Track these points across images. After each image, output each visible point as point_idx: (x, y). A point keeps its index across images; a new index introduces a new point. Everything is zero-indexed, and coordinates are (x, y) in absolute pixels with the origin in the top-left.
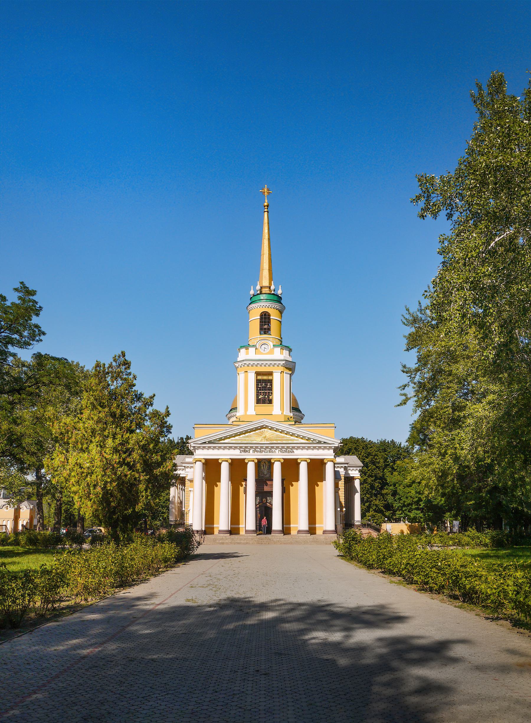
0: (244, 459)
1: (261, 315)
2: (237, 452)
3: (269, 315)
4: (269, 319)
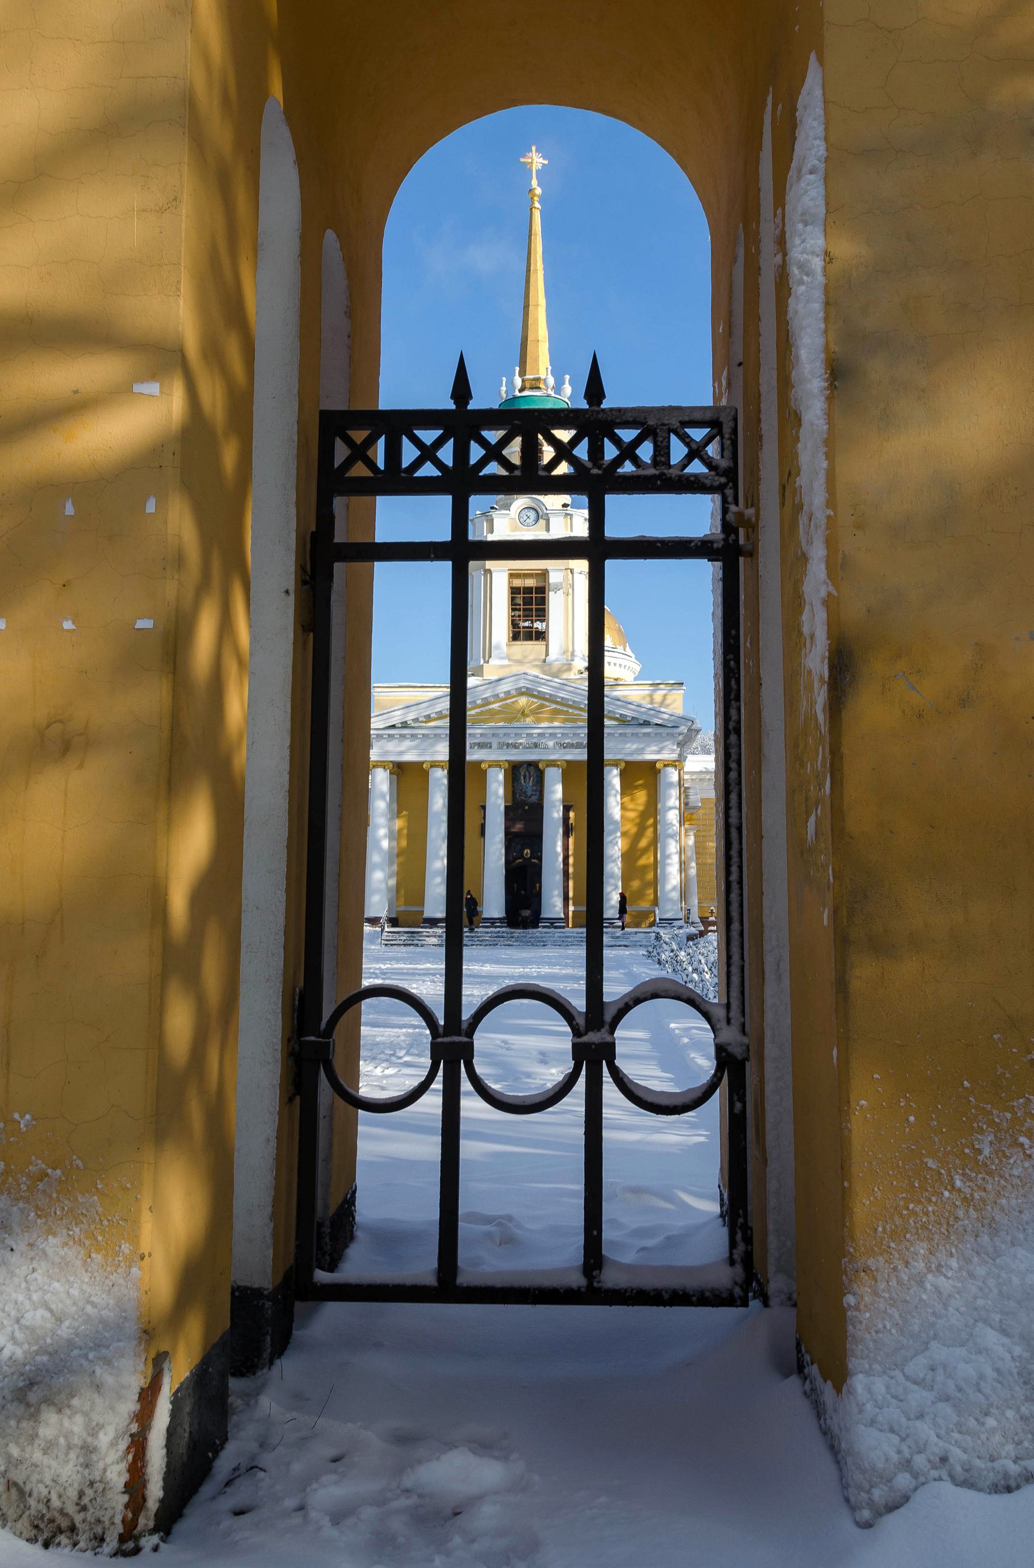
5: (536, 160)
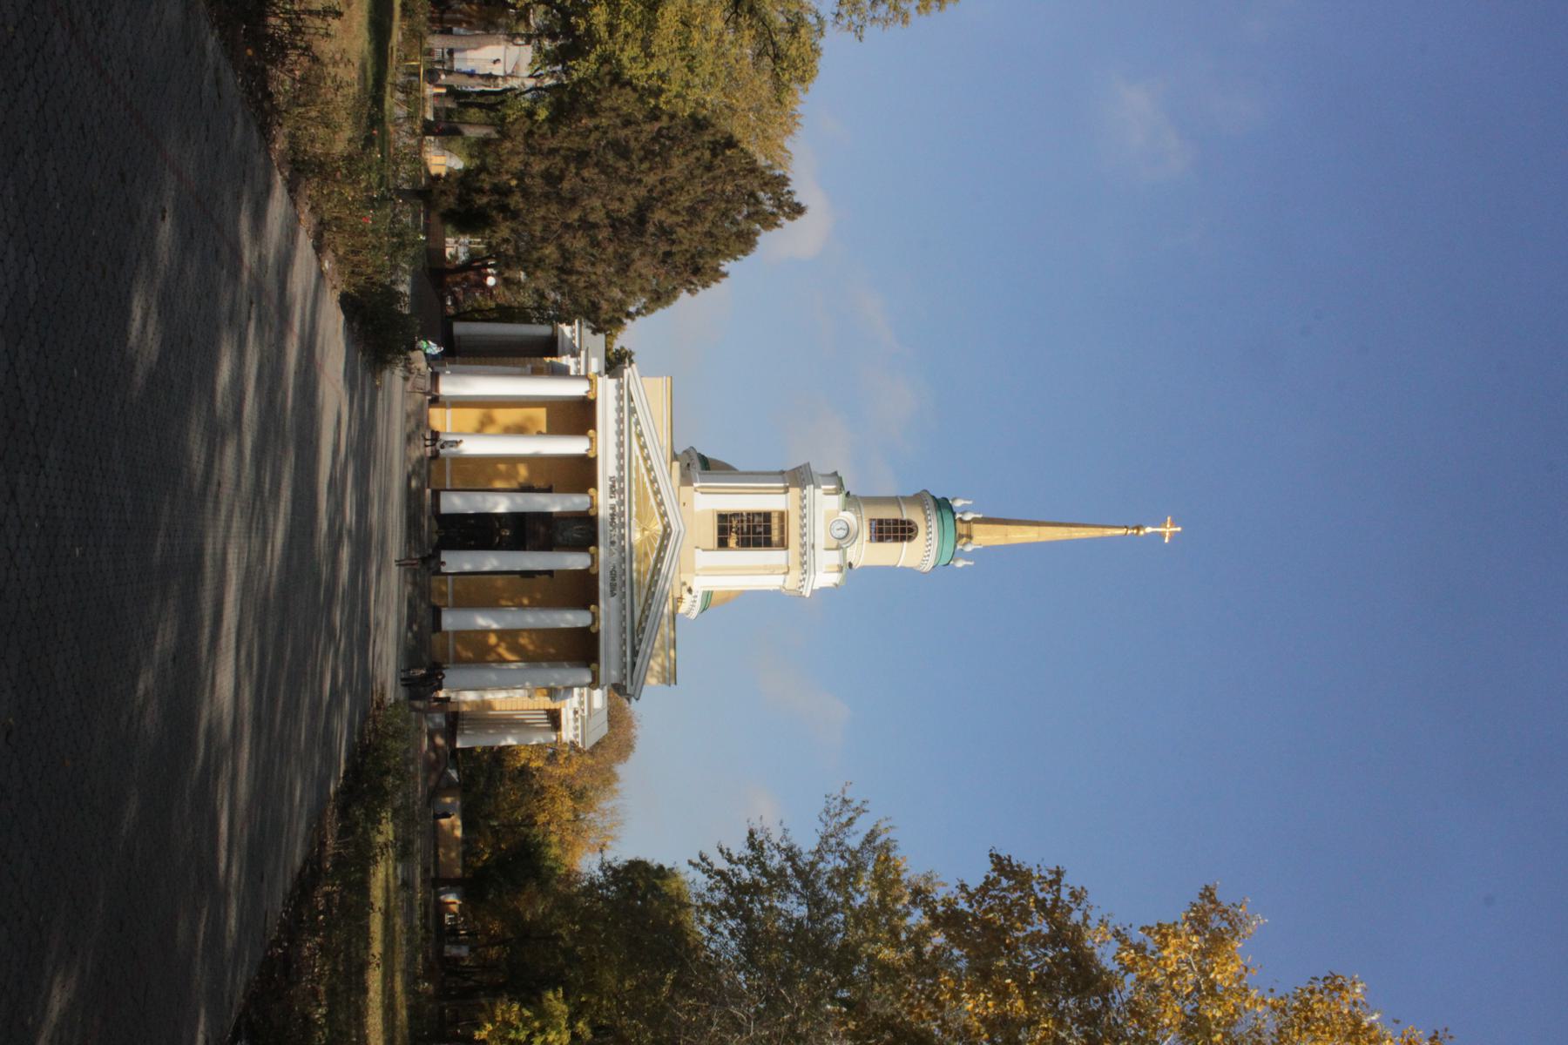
0: (595, 486)
1: (910, 523)
2: (612, 472)
3: (910, 539)
4: (903, 539)
5: (1168, 530)
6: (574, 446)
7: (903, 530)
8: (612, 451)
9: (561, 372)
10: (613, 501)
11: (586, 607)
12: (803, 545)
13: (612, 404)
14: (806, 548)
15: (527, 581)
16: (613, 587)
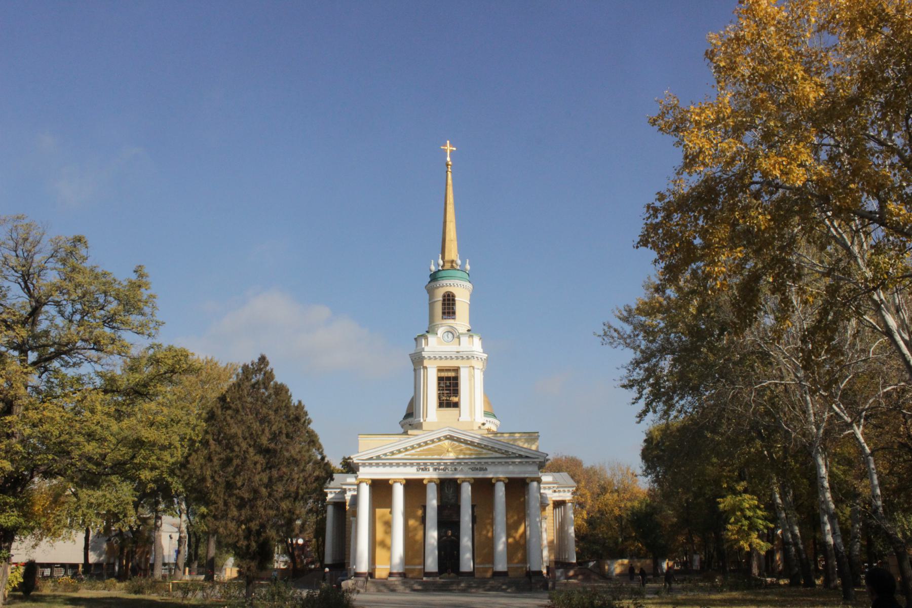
0: (422, 480)
1: (444, 296)
3: (453, 296)
4: (454, 300)
5: (449, 148)
6: (399, 492)
7: (449, 300)
8: (402, 469)
9: (355, 500)
10: (431, 469)
11: (493, 485)
12: (457, 358)
13: (374, 470)
14: (459, 356)
15: (478, 520)
16: (481, 469)
